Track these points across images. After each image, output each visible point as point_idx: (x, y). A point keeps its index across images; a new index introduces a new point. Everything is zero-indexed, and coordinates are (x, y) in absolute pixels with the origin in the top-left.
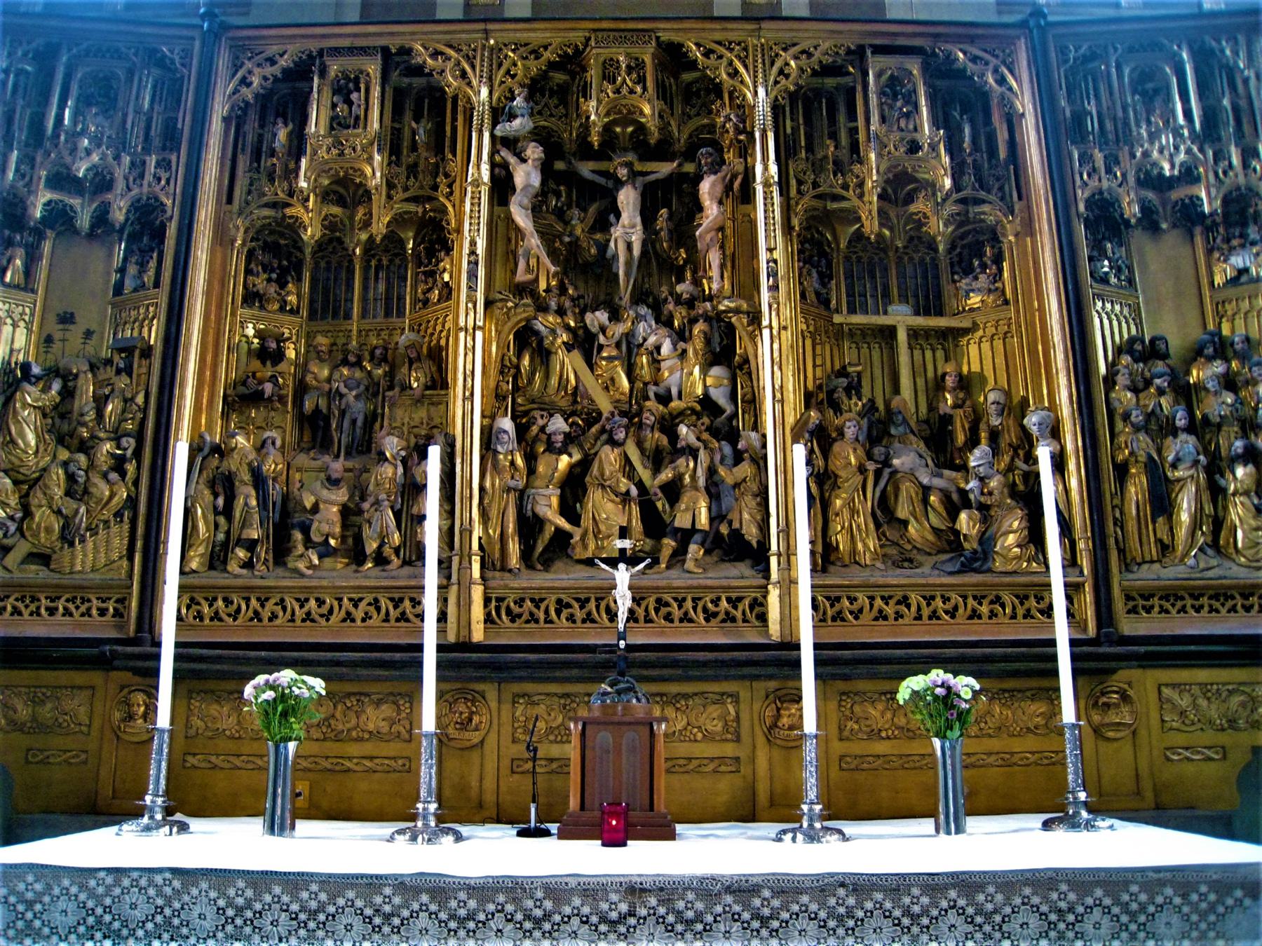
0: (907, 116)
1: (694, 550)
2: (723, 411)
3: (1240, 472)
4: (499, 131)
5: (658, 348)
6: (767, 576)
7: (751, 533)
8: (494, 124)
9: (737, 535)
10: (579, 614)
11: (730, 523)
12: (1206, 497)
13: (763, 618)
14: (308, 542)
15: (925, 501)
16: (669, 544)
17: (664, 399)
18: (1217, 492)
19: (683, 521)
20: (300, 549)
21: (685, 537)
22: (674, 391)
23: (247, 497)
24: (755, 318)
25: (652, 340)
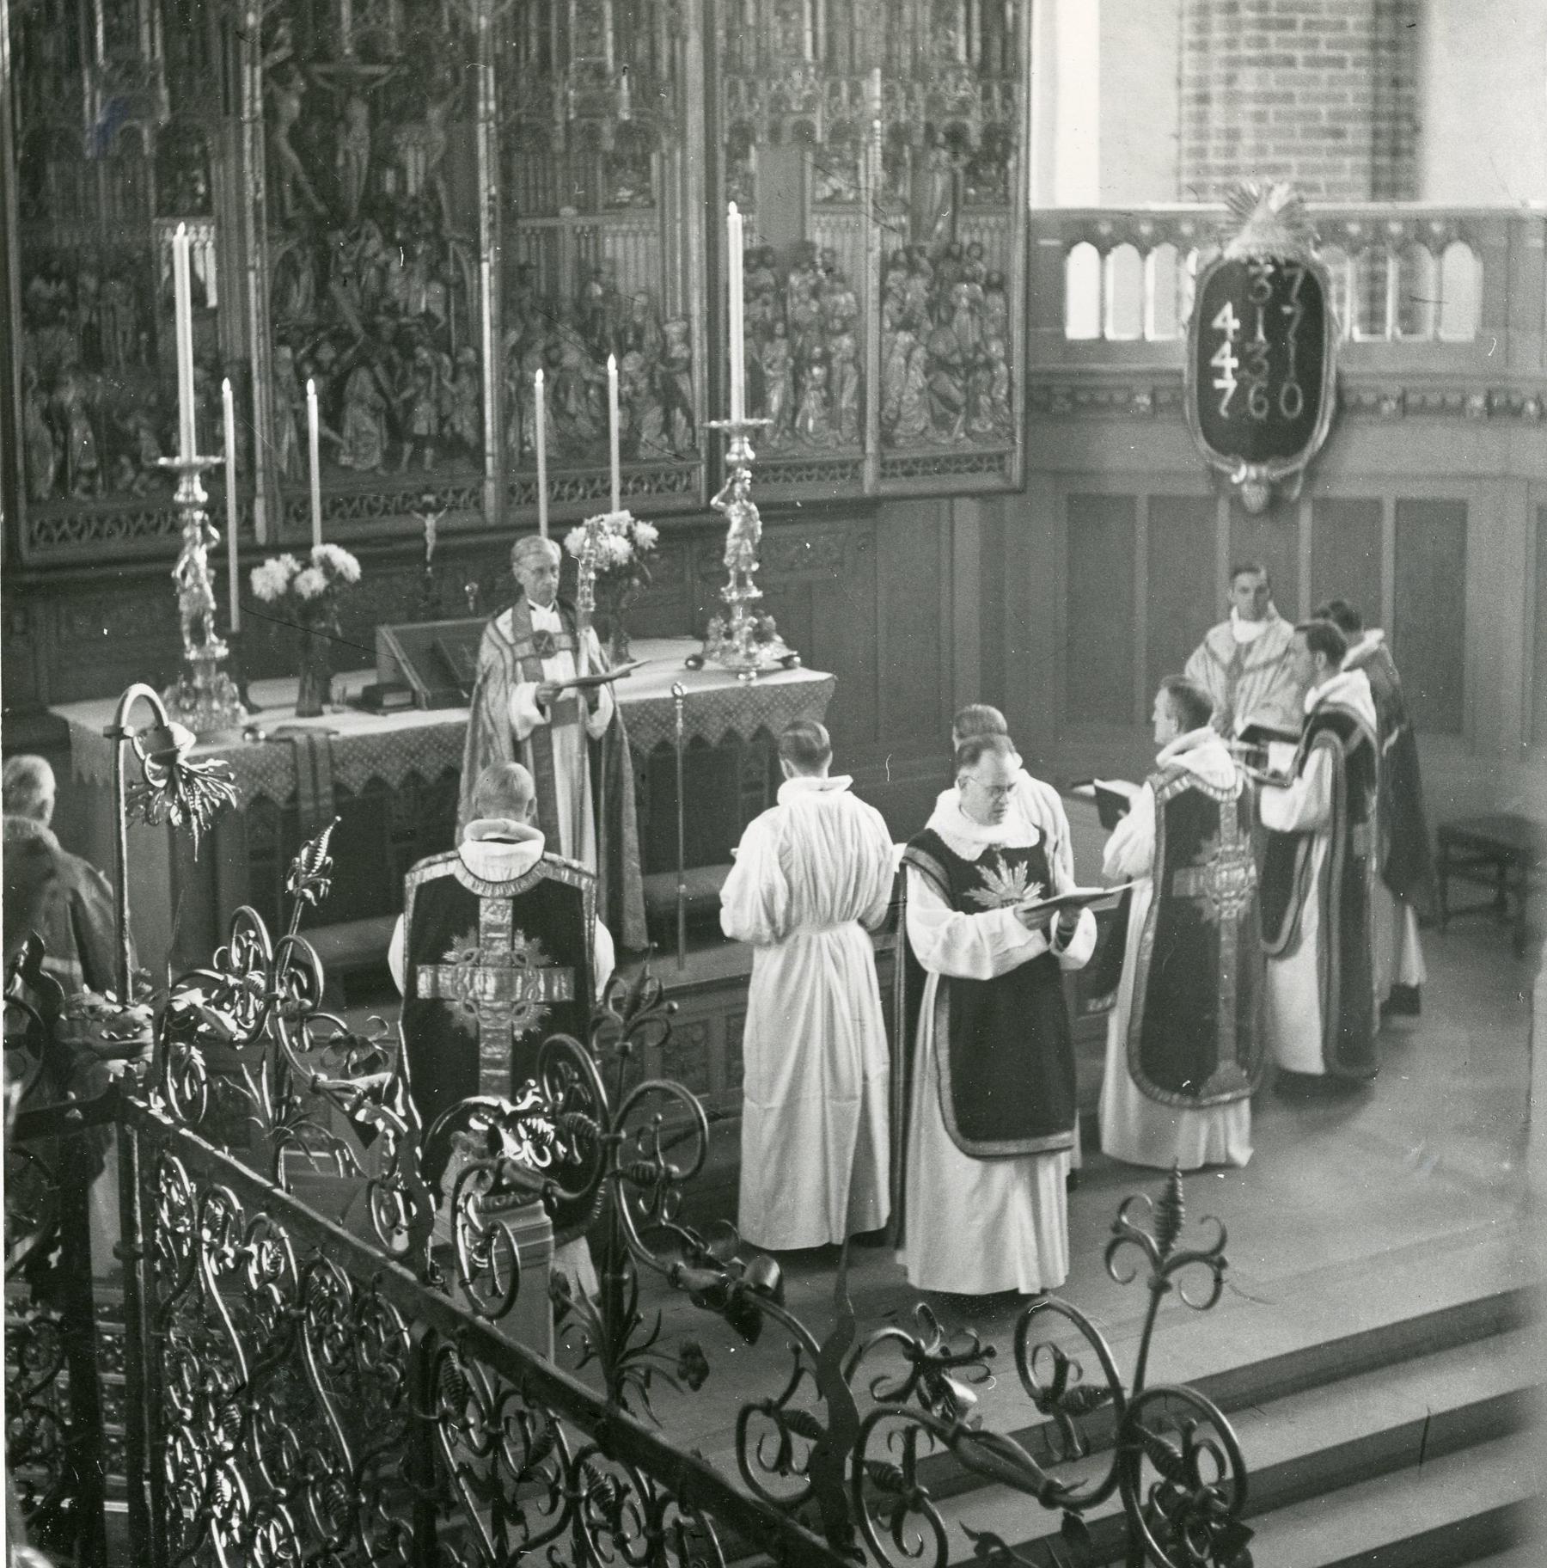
0: (594, 36)
1: (429, 452)
2: (437, 321)
3: (816, 371)
4: (268, 64)
5: (387, 264)
6: (484, 473)
7: (470, 434)
8: (264, 54)
9: (459, 439)
10: (349, 512)
11: (452, 427)
12: (791, 389)
13: (479, 504)
14: (139, 469)
15: (586, 393)
16: (408, 448)
17: (392, 311)
18: (797, 387)
19: (421, 427)
20: (130, 475)
21: (420, 442)
22: (401, 306)
23: (80, 433)
24: (476, 250)
25: (383, 257)
